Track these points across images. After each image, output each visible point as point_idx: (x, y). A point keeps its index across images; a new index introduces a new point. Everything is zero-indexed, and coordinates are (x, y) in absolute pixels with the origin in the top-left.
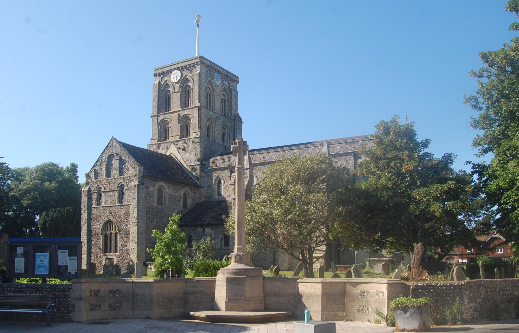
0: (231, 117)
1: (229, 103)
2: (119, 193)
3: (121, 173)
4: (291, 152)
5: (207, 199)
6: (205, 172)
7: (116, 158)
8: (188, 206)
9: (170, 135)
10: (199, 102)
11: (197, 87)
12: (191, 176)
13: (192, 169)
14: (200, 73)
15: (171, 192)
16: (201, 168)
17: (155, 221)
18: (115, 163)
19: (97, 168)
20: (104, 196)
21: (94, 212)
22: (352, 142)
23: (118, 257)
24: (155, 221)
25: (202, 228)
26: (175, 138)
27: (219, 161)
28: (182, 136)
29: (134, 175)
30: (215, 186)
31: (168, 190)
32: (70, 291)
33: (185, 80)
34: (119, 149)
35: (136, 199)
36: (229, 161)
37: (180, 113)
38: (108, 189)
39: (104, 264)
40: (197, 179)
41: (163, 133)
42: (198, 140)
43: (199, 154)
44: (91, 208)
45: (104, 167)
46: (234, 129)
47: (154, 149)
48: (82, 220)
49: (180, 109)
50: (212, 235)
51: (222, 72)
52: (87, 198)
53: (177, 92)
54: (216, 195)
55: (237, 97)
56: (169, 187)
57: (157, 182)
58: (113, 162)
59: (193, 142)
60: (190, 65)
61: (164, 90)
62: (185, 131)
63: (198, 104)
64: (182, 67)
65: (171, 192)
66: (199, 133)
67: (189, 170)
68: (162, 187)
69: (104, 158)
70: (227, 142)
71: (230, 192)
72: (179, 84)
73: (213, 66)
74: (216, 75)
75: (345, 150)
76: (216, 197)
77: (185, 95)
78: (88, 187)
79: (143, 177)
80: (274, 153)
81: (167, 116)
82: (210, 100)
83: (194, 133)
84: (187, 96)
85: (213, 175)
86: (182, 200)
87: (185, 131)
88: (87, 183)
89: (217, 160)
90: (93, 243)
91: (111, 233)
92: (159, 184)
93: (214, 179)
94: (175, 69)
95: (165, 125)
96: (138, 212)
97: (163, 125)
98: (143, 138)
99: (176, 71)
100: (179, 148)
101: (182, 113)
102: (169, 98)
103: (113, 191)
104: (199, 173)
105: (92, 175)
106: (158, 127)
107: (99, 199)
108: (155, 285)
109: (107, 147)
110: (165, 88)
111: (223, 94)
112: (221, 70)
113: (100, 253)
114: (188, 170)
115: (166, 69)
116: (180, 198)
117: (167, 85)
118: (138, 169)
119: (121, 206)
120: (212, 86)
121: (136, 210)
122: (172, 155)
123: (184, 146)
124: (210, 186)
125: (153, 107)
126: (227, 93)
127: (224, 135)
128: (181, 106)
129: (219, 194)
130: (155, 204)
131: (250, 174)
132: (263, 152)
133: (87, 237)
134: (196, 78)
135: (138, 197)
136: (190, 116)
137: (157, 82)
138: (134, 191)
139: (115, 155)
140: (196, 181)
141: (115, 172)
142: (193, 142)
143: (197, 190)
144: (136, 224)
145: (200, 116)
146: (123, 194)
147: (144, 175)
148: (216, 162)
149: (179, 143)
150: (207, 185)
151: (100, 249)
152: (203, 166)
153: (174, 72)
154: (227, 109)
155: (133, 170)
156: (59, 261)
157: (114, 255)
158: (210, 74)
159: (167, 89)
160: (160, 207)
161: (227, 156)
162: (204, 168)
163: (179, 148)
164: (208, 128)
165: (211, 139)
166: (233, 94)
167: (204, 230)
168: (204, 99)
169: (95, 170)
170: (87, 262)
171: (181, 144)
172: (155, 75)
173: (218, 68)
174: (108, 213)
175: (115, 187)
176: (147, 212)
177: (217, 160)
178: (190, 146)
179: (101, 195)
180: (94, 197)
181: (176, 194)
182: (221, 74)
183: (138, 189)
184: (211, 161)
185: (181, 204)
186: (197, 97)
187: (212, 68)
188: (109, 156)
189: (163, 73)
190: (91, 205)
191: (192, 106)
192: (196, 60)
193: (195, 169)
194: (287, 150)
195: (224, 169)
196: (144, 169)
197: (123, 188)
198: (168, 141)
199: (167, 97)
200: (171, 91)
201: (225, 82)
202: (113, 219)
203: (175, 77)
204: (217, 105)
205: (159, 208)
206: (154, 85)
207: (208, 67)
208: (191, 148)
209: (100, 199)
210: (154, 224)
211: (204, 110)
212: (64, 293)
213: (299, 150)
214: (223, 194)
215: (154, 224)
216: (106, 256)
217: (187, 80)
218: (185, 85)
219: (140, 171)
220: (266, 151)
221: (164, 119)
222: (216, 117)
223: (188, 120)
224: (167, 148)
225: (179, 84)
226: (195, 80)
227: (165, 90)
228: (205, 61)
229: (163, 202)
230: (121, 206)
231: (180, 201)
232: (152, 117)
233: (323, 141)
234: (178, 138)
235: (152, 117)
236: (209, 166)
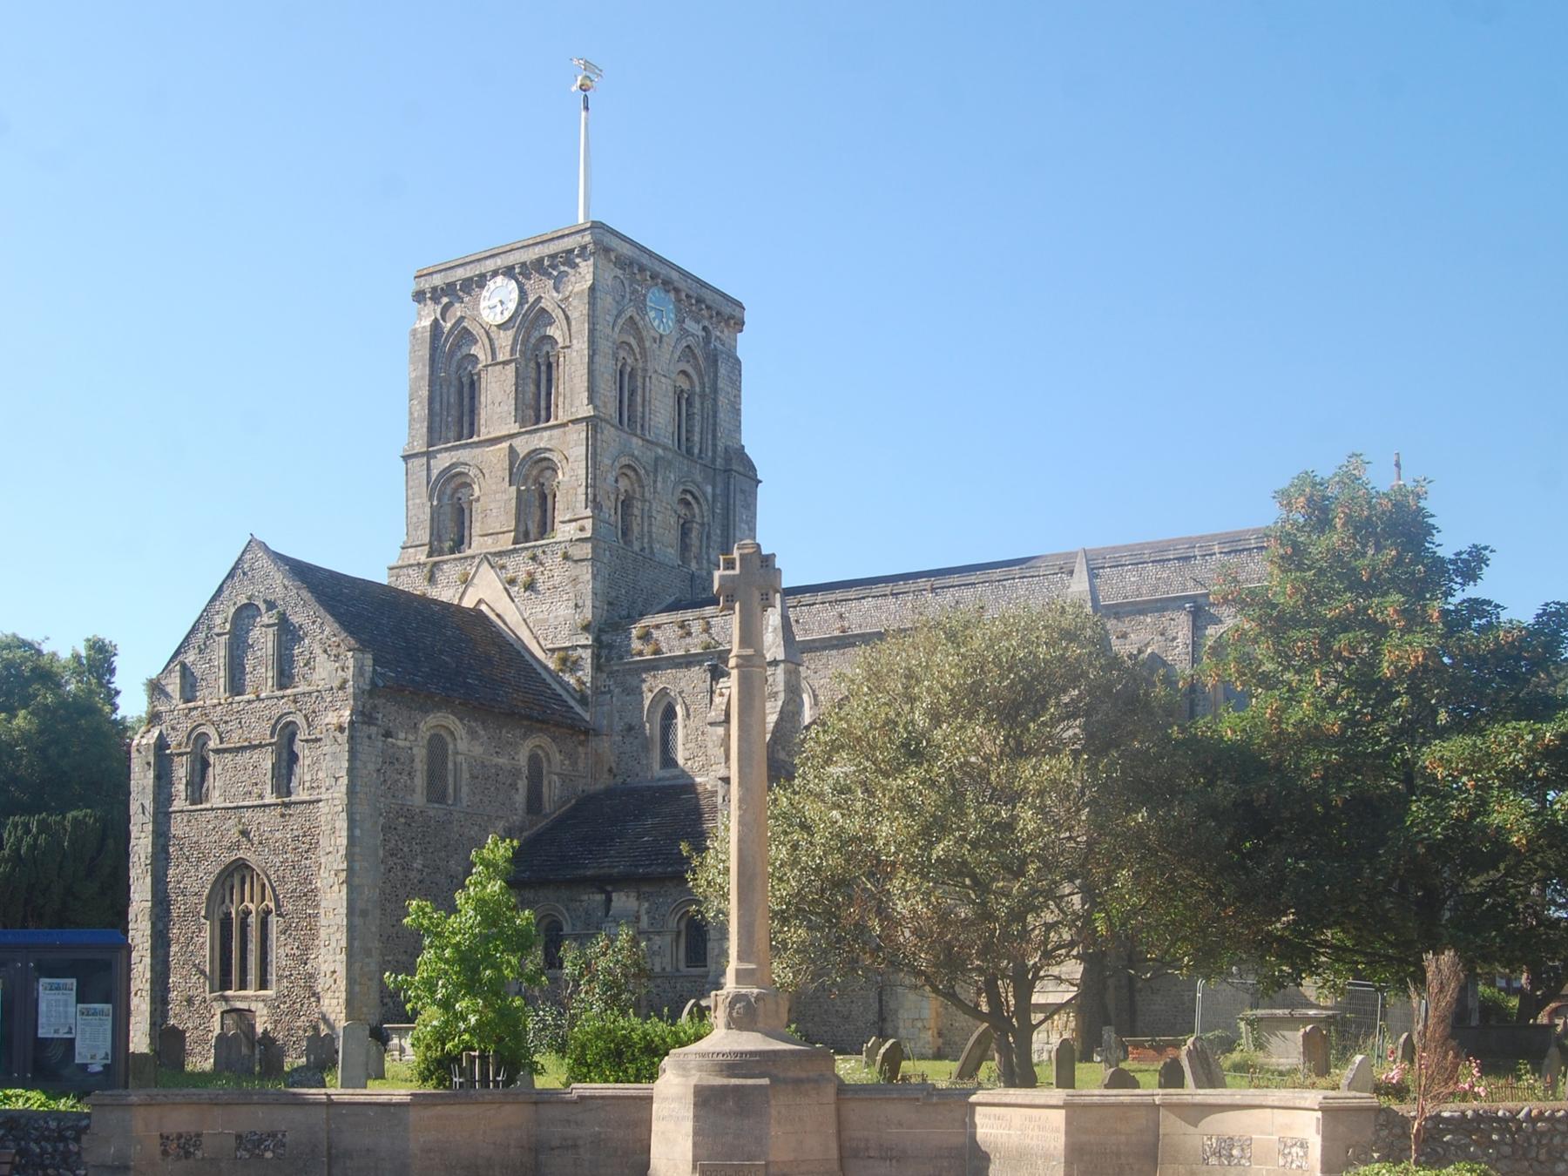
0: (714, 460)
1: (708, 404)
2: (279, 756)
3: (284, 678)
4: (949, 597)
5: (619, 780)
6: (611, 674)
7: (265, 620)
8: (548, 807)
9: (477, 528)
10: (591, 400)
11: (581, 345)
12: (559, 690)
13: (564, 661)
14: (592, 289)
15: (478, 750)
16: (596, 657)
17: (418, 864)
18: (263, 639)
19: (190, 657)
20: (218, 769)
21: (178, 827)
22: (1187, 559)
24: (418, 864)
25: (602, 891)
26: (495, 543)
27: (666, 632)
28: (522, 535)
29: (336, 684)
30: (651, 728)
31: (468, 744)
32: (84, 1138)
33: (537, 317)
34: (278, 585)
35: (344, 781)
36: (707, 630)
37: (516, 442)
38: (235, 740)
39: (217, 1031)
40: (583, 700)
41: (449, 524)
42: (587, 550)
43: (589, 603)
44: (168, 815)
45: (219, 654)
46: (727, 509)
47: (413, 584)
48: (133, 859)
49: (515, 428)
50: (638, 918)
51: (681, 285)
52: (151, 774)
53: (505, 363)
54: (656, 766)
55: (736, 383)
56: (473, 734)
57: (427, 712)
58: (255, 633)
59: (566, 557)
60: (553, 257)
61: (452, 353)
62: (535, 514)
64: (523, 264)
65: (478, 750)
66: (588, 524)
67: (552, 666)
69: (218, 620)
70: (699, 559)
71: (708, 752)
72: (511, 333)
73: (645, 260)
74: (654, 296)
75: (1156, 589)
76: (657, 770)
77: (533, 375)
78: (156, 732)
79: (371, 693)
80: (880, 601)
81: (463, 455)
82: (632, 393)
83: (572, 521)
84: (544, 377)
85: (645, 687)
86: (522, 784)
87: (535, 514)
88: (154, 718)
89: (658, 627)
90: (174, 949)
91: (247, 913)
92: (430, 722)
93: (647, 703)
94: (495, 273)
95: (456, 490)
96: (351, 829)
97: (449, 491)
98: (373, 541)
99: (500, 279)
100: (512, 582)
101: (523, 446)
102: (472, 384)
103: (256, 747)
104: (587, 679)
105: (173, 686)
106: (431, 499)
107: (198, 779)
108: (413, 1115)
109: (231, 575)
110: (457, 346)
111: (684, 372)
112: (674, 275)
113: (203, 990)
114: (546, 668)
115: (461, 273)
116: (515, 773)
117: (466, 336)
118: (350, 663)
119: (285, 805)
120: (641, 340)
121: (342, 824)
122: (483, 607)
123: (530, 574)
124: (630, 728)
125: (412, 420)
126: (697, 367)
127: (685, 531)
128: (521, 419)
129: (669, 761)
130: (418, 799)
131: (787, 683)
132: (838, 595)
133: (154, 925)
134: (579, 310)
135: (350, 771)
136: (555, 457)
137: (427, 322)
138: (336, 748)
139: (263, 607)
140: (578, 709)
141: (260, 672)
142: (566, 557)
143: (581, 743)
144: (343, 875)
145: (593, 457)
146: (293, 758)
147: (373, 684)
148: (656, 633)
149: (510, 562)
150: (619, 726)
151: (203, 972)
152: (604, 652)
153: (491, 284)
154: (697, 429)
155: (331, 666)
156: (42, 1020)
157: (257, 998)
158: (634, 292)
159: (465, 351)
160: (435, 810)
161: (697, 612)
162: (608, 660)
163: (512, 582)
164: (626, 504)
165: (636, 547)
166: (722, 371)
167: (609, 900)
168: (608, 389)
169: (184, 666)
170: (153, 1024)
171: (519, 566)
172: (419, 296)
173: (664, 271)
174: (234, 835)
175: (261, 731)
176: (386, 829)
177: (658, 627)
178: (554, 571)
179: (205, 765)
180: (181, 772)
181: (501, 761)
182: (677, 290)
183: (351, 738)
184: (634, 632)
185: (520, 798)
187: (642, 269)
188: (239, 610)
189: (449, 290)
190: (170, 800)
191: (562, 418)
192: (578, 238)
193: (575, 663)
194: (933, 590)
195: (687, 661)
196: (376, 661)
197: (294, 734)
198: (469, 552)
200: (481, 356)
201: (690, 325)
202: (252, 858)
203: (497, 302)
204: (662, 415)
205: (431, 813)
206: (414, 332)
207: (623, 263)
208: (557, 580)
209: (203, 779)
210: (412, 875)
211: (609, 433)
212: (61, 1146)
213: (980, 588)
214: (681, 762)
215: (412, 875)
216: (226, 999)
217: (543, 317)
218: (536, 334)
219: (360, 671)
220: (852, 594)
221: (453, 466)
222: (657, 459)
223: (548, 473)
224: (466, 581)
225: (511, 333)
226: (574, 315)
227: (459, 355)
228: (614, 243)
229: (451, 790)
230: (285, 805)
231: (513, 786)
232: (406, 458)
233: (1073, 555)
234: (506, 542)
235: (406, 458)
236: (629, 652)
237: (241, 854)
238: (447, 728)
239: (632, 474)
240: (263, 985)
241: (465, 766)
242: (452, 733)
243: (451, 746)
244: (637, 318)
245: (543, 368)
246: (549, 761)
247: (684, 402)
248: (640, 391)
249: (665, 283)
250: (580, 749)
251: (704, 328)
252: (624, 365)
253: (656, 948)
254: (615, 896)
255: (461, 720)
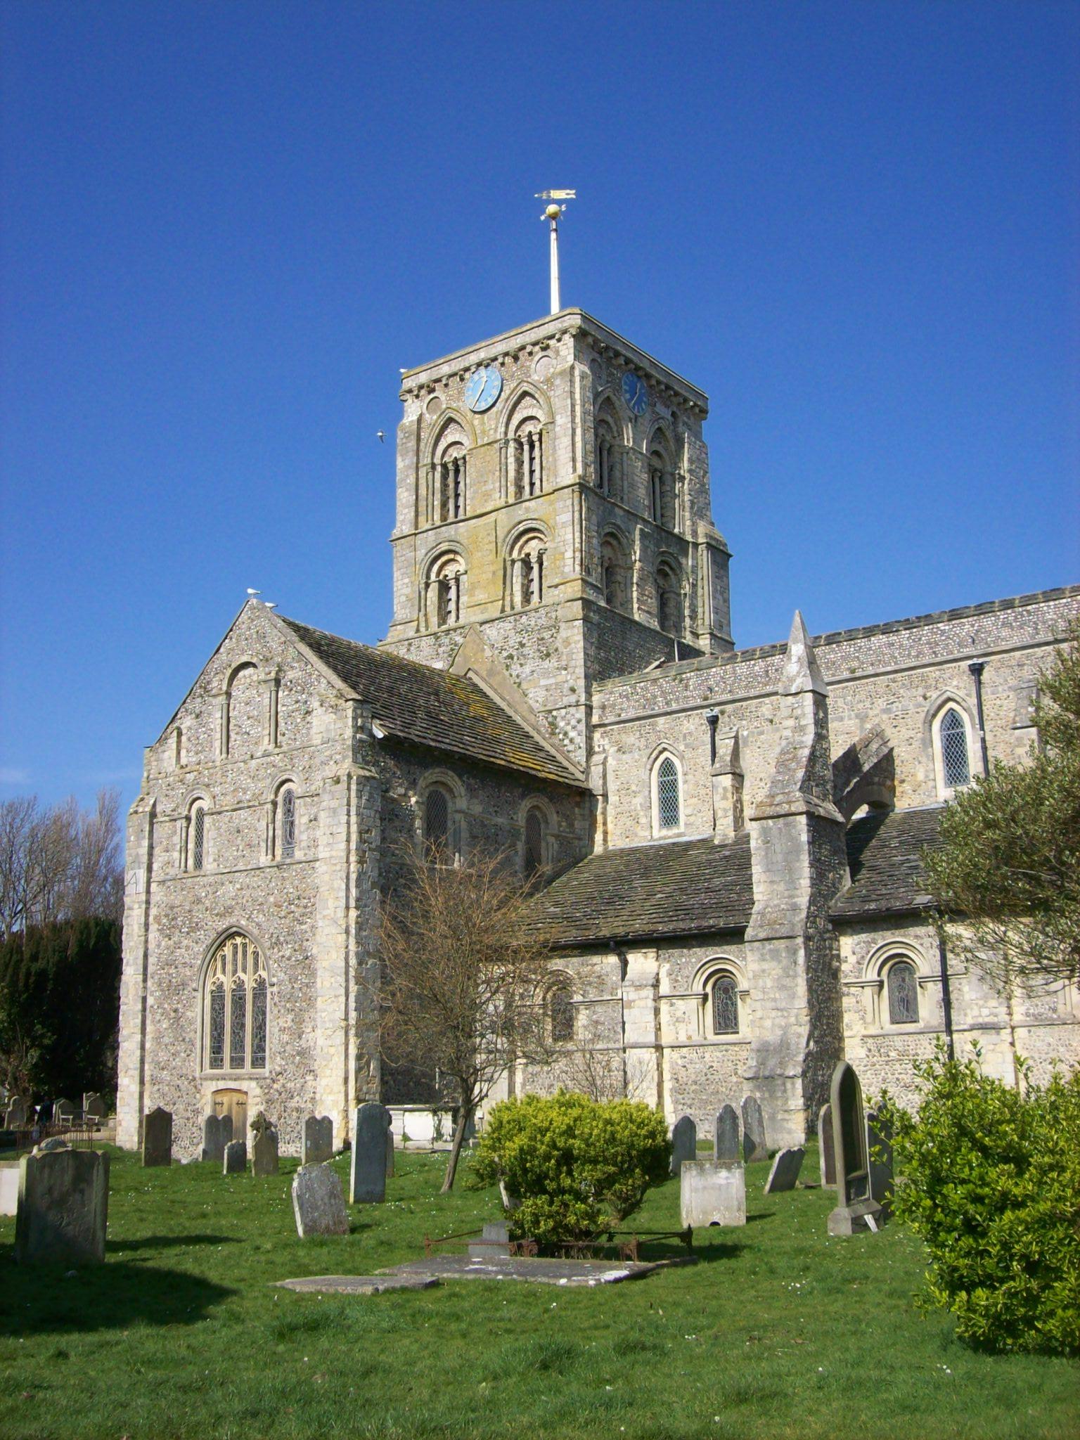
11: (562, 420)
15: (477, 809)
23: (266, 1085)
39: (208, 1112)
56: (471, 791)
57: (426, 767)
63: (570, 478)
65: (477, 809)
68: (441, 789)
82: (611, 469)
91: (240, 985)
111: (656, 453)
116: (514, 834)
122: (470, 674)
143: (578, 805)
158: (611, 374)
167: (625, 963)
182: (648, 376)
186: (564, 454)
199: (450, 466)
237: (233, 920)
238: (443, 784)
239: (614, 542)
240: (258, 1061)
241: (464, 825)
242: (450, 791)
243: (450, 804)
244: (614, 398)
245: (526, 447)
246: (547, 822)
247: (657, 480)
248: (618, 466)
249: (638, 368)
250: (577, 810)
251: (673, 414)
252: (603, 441)
253: (679, 1014)
254: (631, 957)
255: (460, 777)
